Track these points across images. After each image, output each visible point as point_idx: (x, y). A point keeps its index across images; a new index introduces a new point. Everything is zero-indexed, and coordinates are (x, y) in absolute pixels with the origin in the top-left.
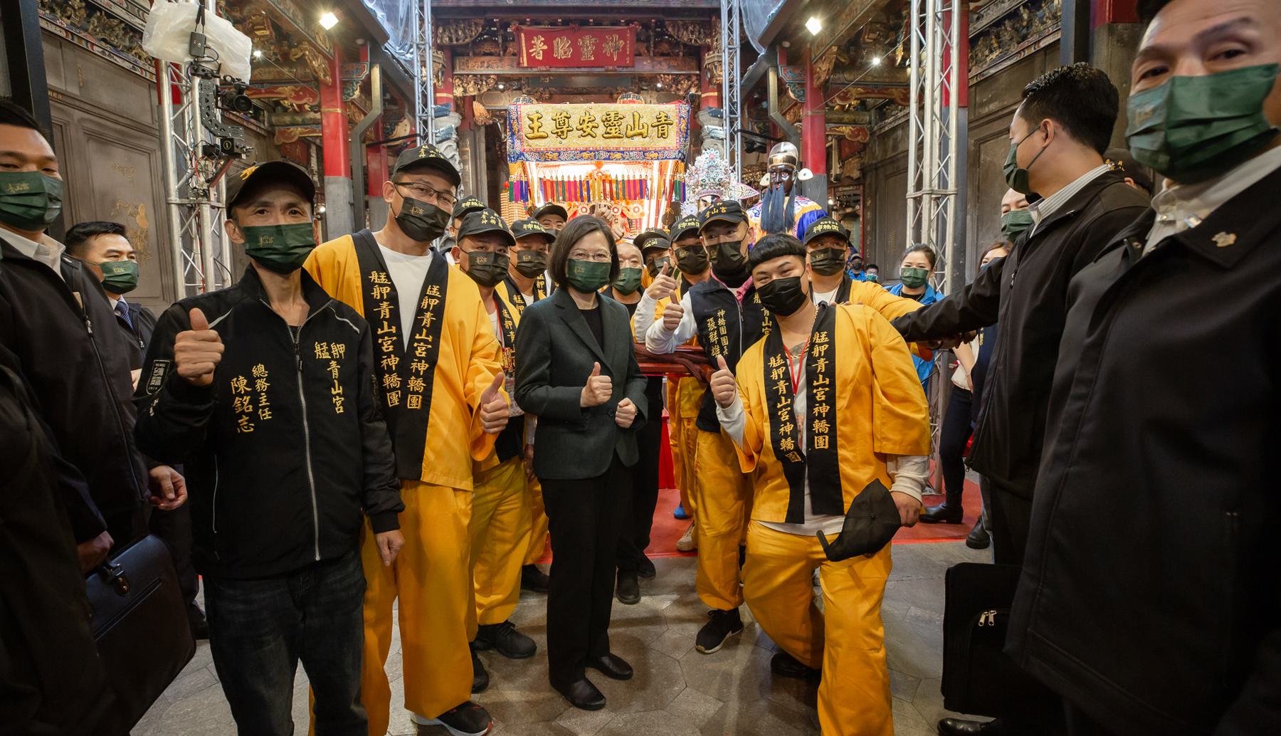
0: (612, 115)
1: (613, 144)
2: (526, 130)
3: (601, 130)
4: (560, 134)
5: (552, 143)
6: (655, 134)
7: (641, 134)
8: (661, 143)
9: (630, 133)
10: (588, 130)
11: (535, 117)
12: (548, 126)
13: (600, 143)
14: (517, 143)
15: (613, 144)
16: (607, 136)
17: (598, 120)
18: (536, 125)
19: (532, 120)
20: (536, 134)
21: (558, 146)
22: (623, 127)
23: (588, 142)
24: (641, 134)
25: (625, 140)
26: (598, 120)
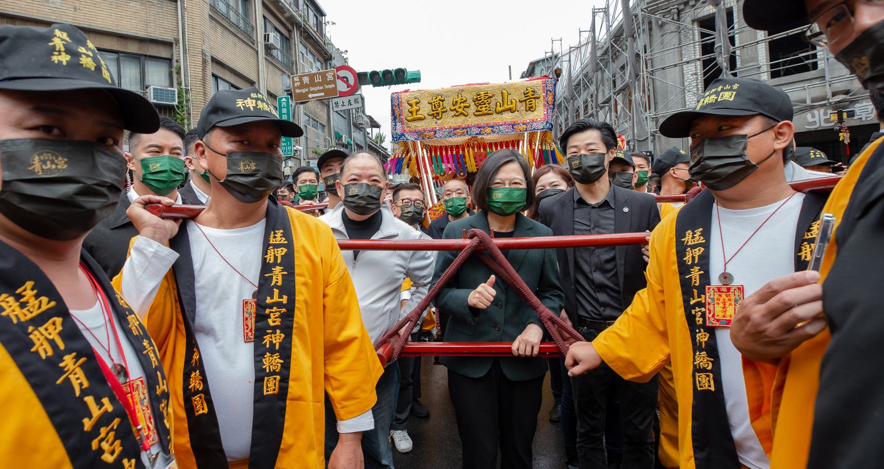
2: (406, 113)
3: (473, 109)
4: (435, 116)
5: (429, 124)
6: (523, 108)
7: (510, 110)
9: (499, 109)
10: (460, 110)
11: (413, 101)
12: (425, 109)
13: (472, 120)
14: (399, 125)
17: (470, 102)
18: (415, 108)
19: (411, 105)
20: (415, 116)
21: (434, 125)
22: (493, 102)
23: (460, 121)
25: (495, 115)
26: (470, 102)
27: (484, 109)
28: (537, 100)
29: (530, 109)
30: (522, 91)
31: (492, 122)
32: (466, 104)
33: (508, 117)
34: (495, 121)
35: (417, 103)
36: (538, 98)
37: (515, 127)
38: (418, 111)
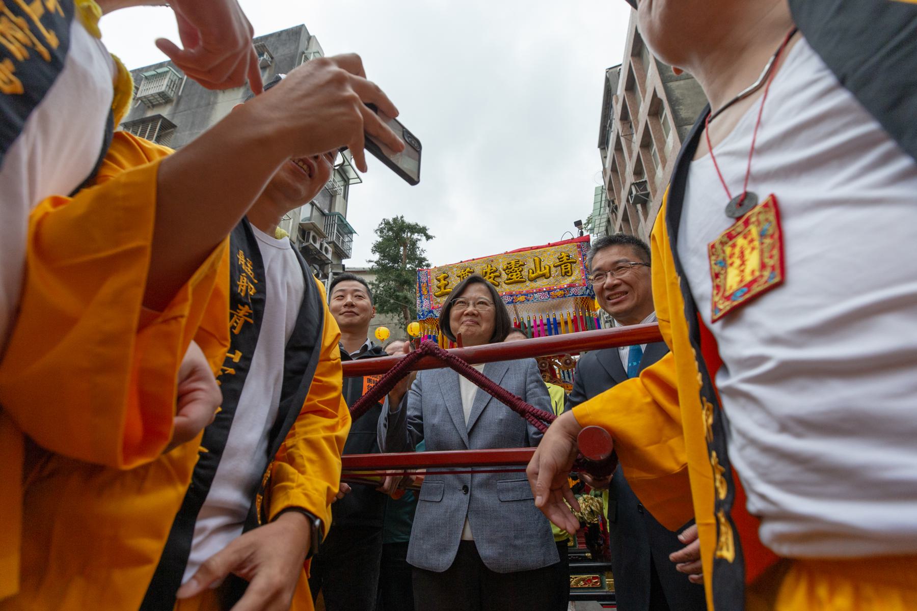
0: (513, 263)
1: (515, 288)
2: (434, 289)
8: (568, 281)
9: (533, 276)
15: (515, 288)
16: (510, 282)
19: (439, 280)
22: (526, 270)
24: (544, 275)
25: (528, 283)
27: (514, 277)
28: (574, 265)
29: (566, 274)
30: (556, 256)
31: (525, 290)
32: (497, 274)
33: (542, 283)
34: (527, 289)
35: (445, 278)
36: (575, 263)
37: (552, 293)
38: (446, 286)
